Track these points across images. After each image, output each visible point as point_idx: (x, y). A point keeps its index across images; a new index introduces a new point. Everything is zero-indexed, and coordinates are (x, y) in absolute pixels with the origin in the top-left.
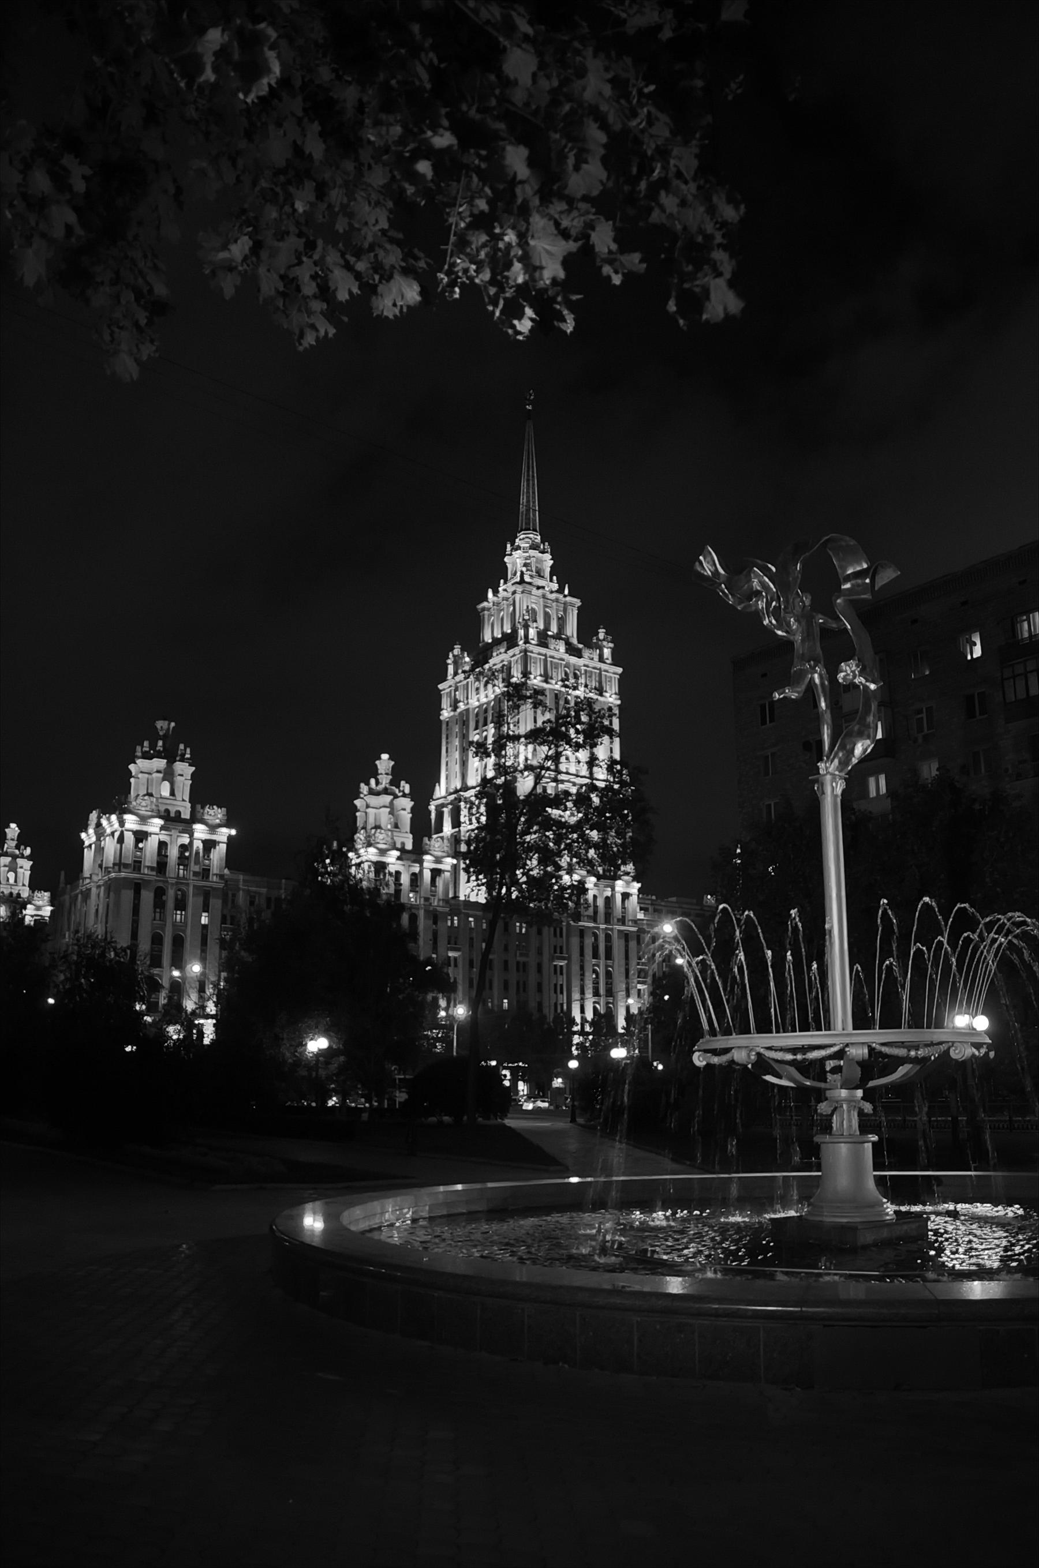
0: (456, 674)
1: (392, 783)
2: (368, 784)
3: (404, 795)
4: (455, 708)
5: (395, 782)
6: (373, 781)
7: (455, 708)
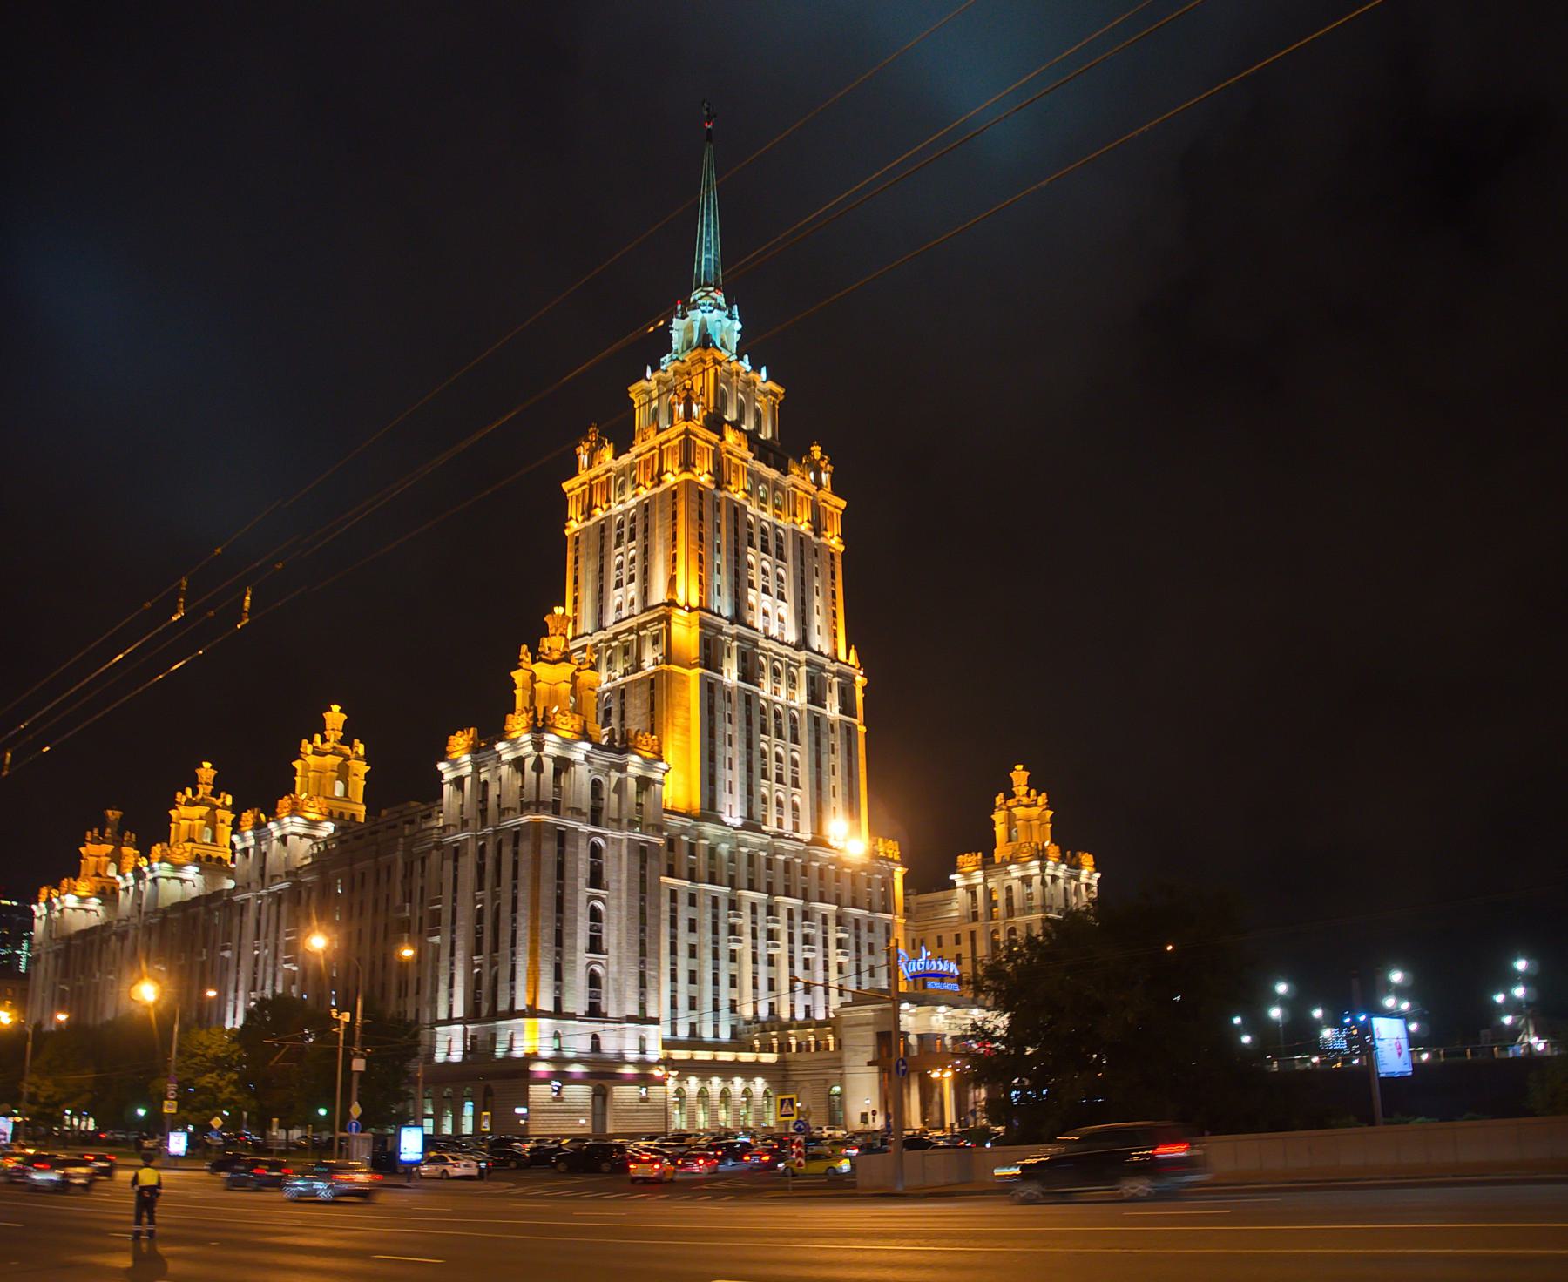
0: (590, 466)
1: (342, 741)
2: (311, 742)
3: (358, 758)
4: (588, 512)
5: (346, 740)
6: (318, 737)
7: (588, 512)
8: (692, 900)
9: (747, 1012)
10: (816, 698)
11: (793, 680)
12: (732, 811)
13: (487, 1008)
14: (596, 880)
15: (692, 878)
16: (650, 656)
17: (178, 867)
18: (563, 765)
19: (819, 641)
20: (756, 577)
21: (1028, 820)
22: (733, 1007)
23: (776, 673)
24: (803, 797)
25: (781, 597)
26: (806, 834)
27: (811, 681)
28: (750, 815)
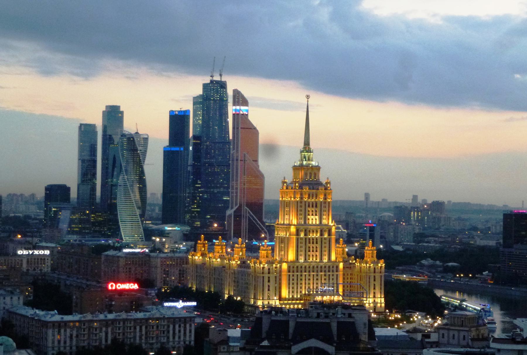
8: (293, 275)
9: (303, 292)
10: (322, 235)
11: (317, 232)
12: (302, 260)
13: (255, 298)
14: (269, 281)
15: (293, 272)
16: (288, 234)
17: (216, 259)
18: (263, 268)
19: (324, 222)
20: (311, 214)
21: (369, 253)
22: (301, 292)
23: (313, 231)
24: (318, 254)
25: (316, 215)
26: (318, 260)
27: (321, 231)
28: (305, 259)
